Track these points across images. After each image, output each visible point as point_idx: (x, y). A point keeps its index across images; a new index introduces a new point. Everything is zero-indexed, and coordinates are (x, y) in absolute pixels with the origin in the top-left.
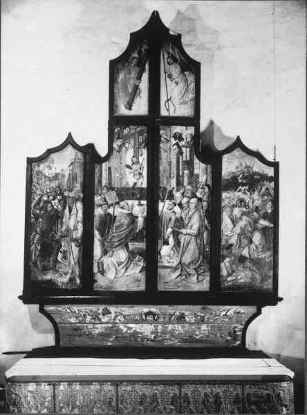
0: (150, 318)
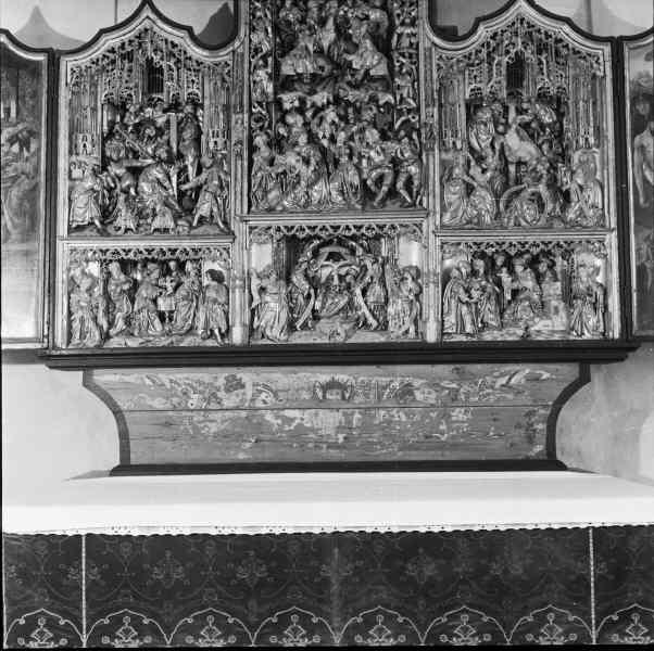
0: (333, 396)
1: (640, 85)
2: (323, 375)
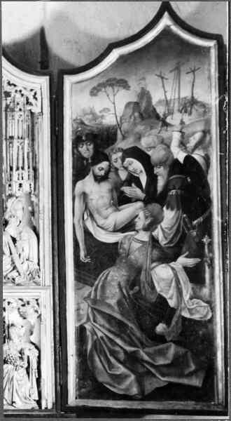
1: (82, 123)
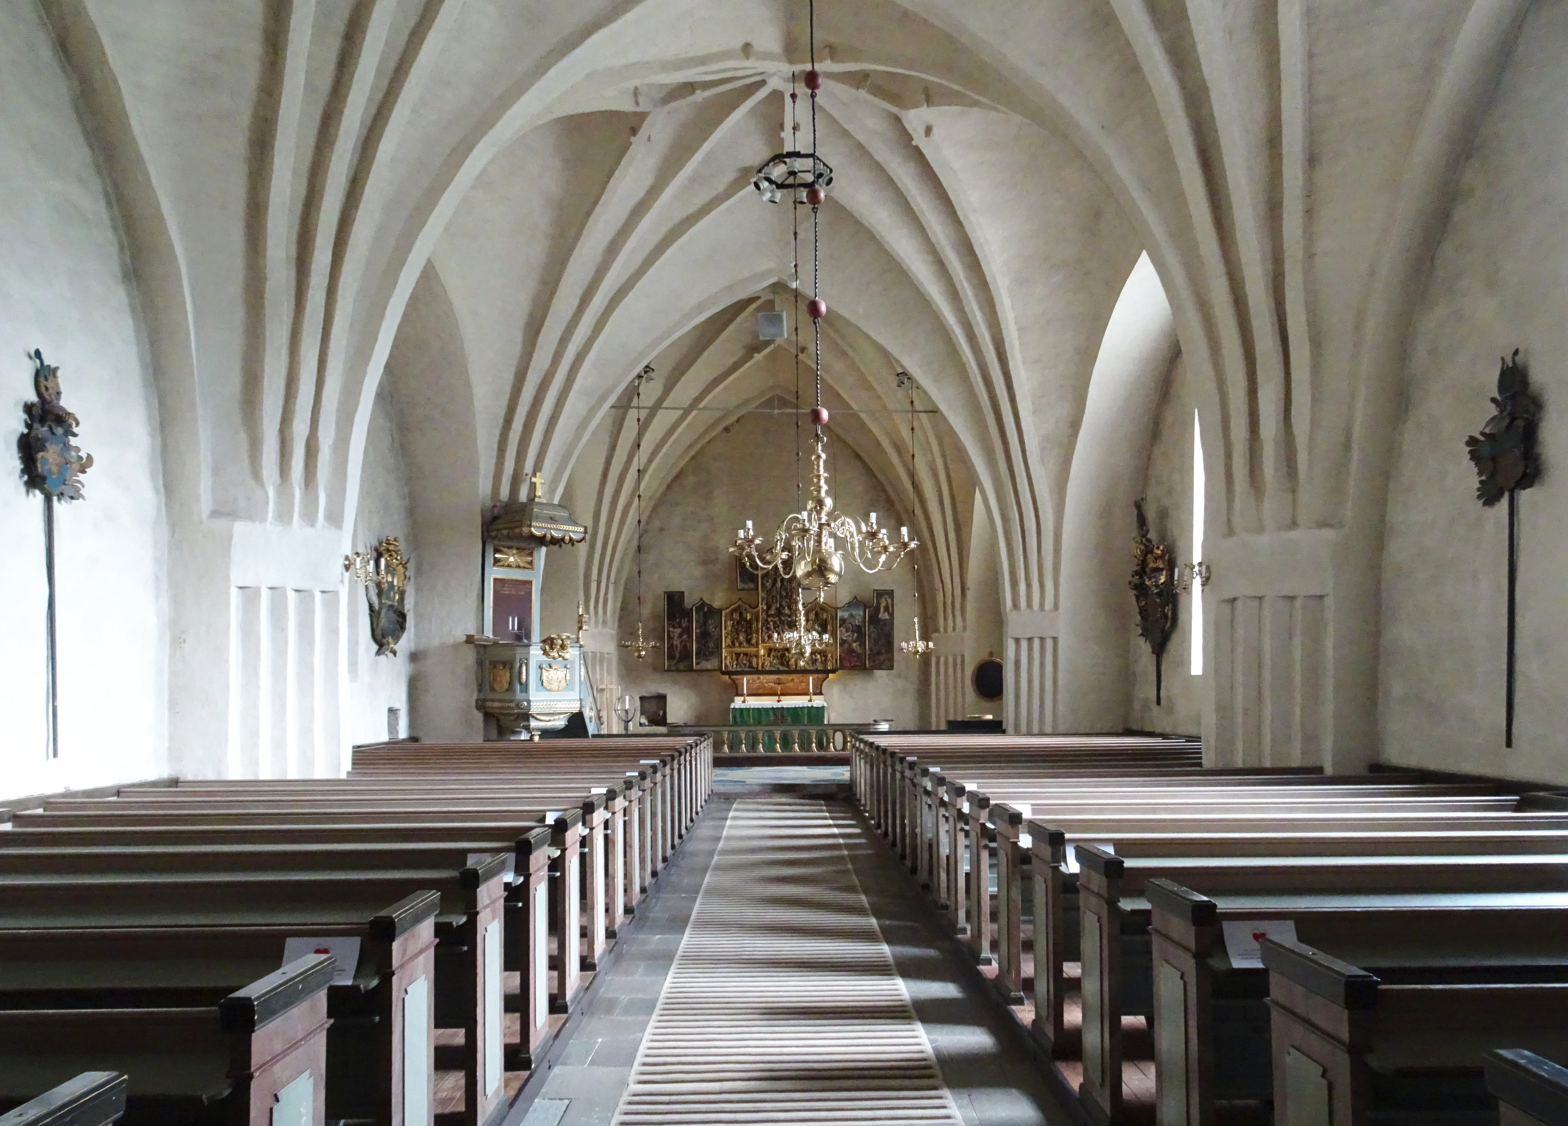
2: (776, 677)
